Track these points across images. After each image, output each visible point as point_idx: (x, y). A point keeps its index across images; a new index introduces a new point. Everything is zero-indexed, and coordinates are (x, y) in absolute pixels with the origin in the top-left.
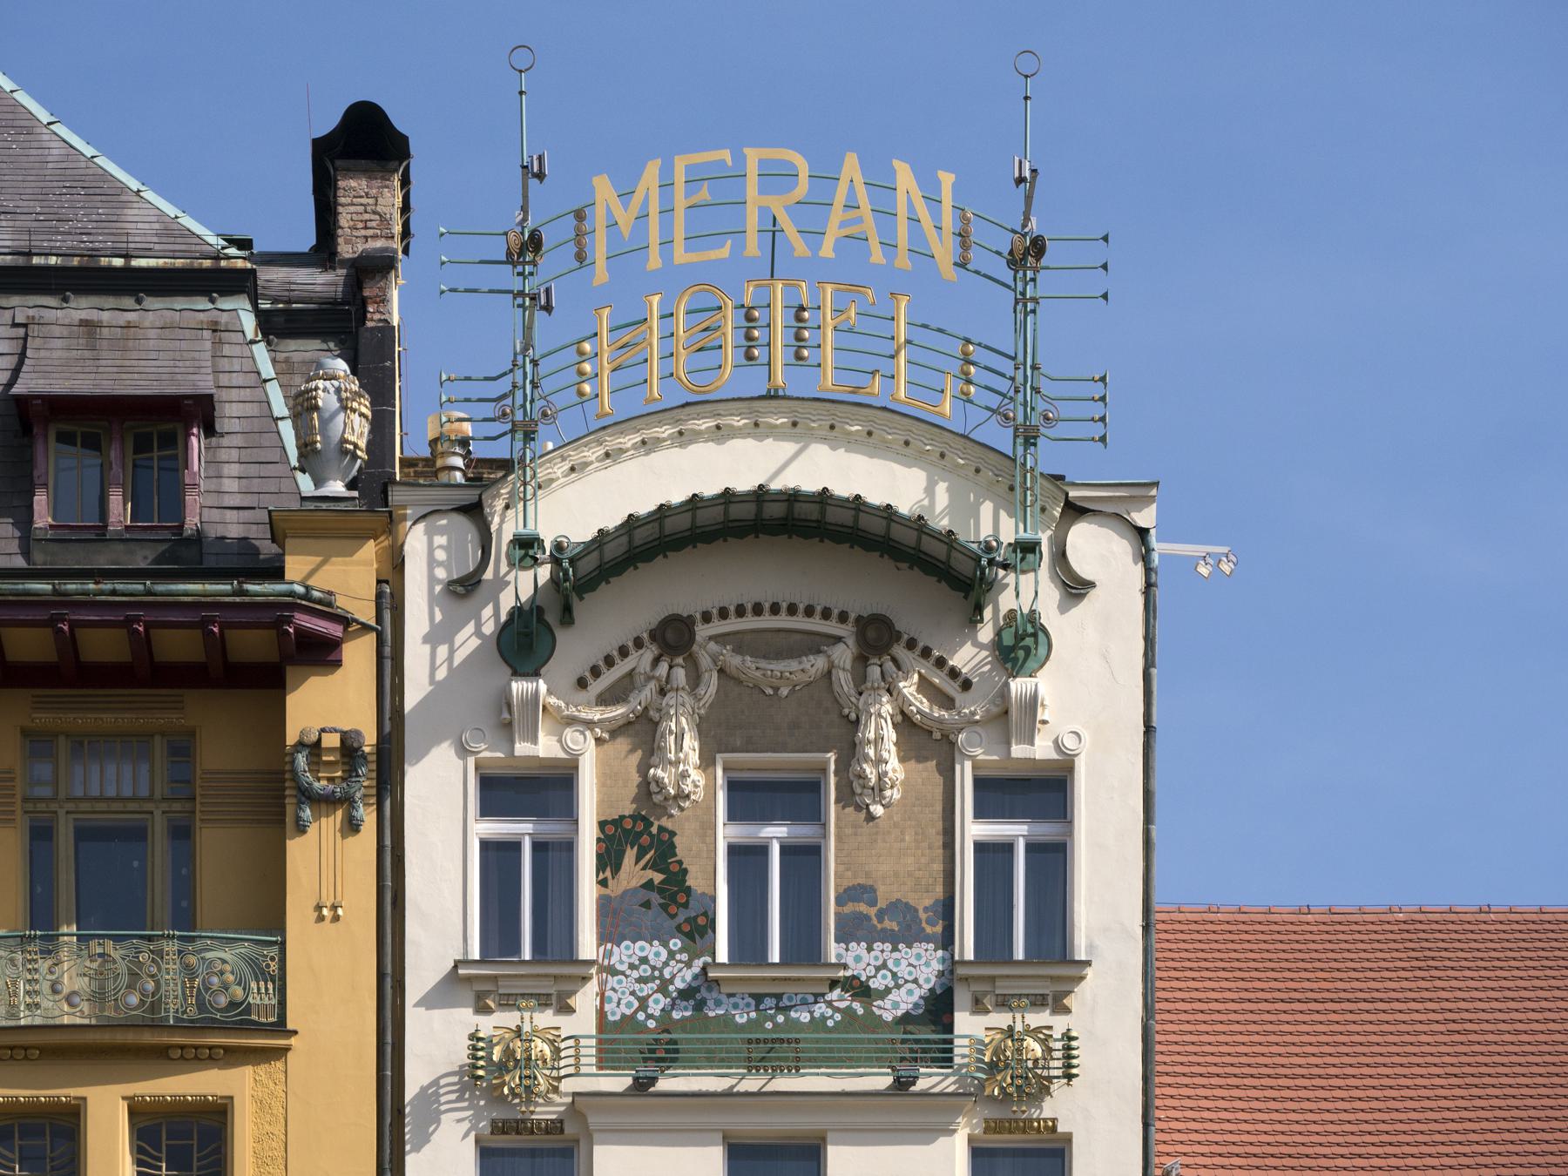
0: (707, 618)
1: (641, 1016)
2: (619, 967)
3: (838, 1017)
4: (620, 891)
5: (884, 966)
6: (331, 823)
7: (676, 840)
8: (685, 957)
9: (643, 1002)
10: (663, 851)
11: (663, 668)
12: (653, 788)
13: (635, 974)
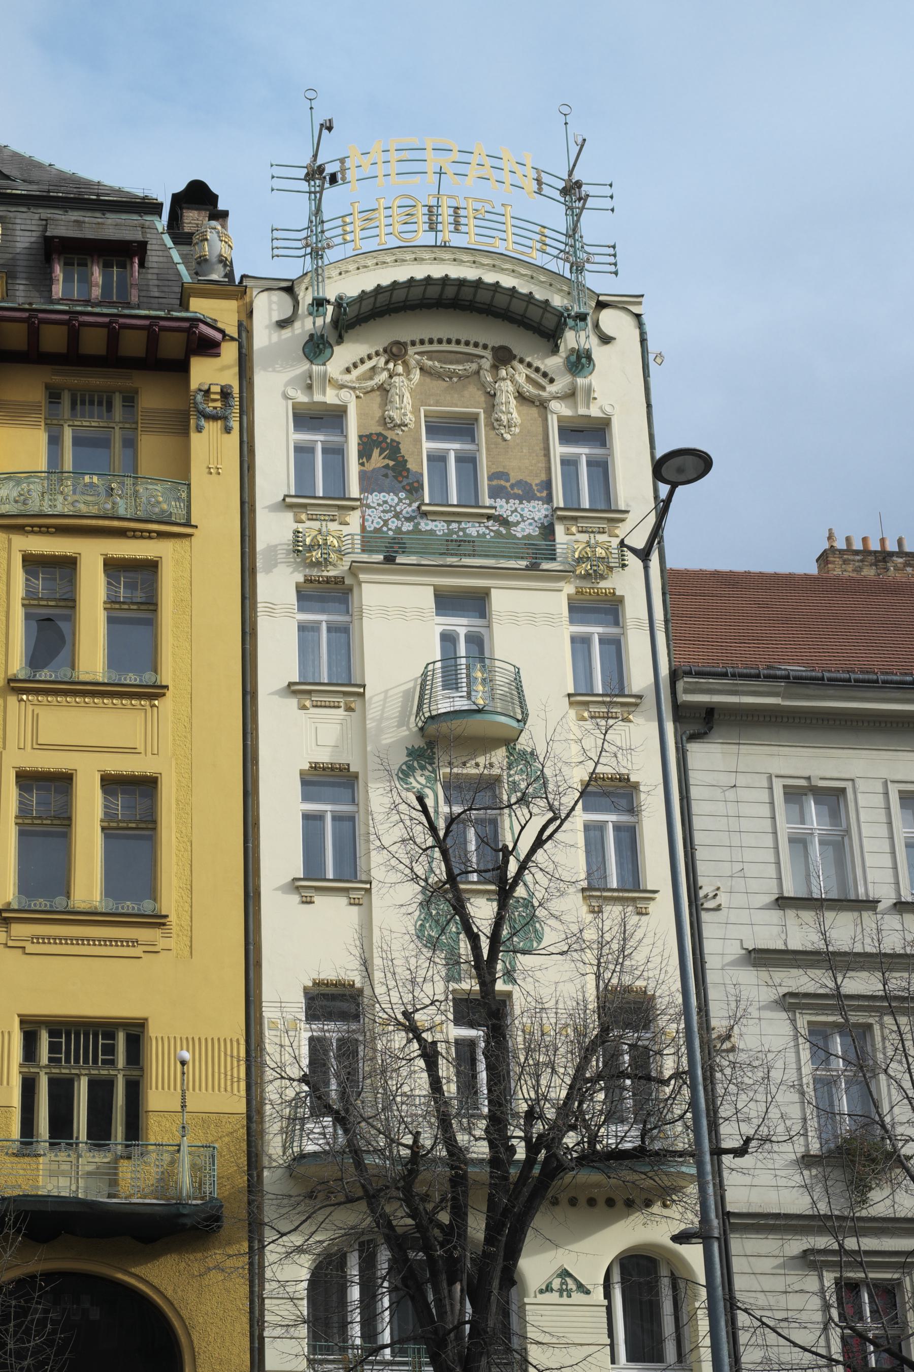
0: (413, 343)
1: (385, 529)
2: (372, 504)
3: (492, 534)
4: (371, 469)
5: (516, 510)
6: (213, 428)
7: (401, 446)
8: (407, 501)
9: (386, 522)
10: (393, 450)
11: (391, 365)
12: (388, 420)
13: (381, 509)
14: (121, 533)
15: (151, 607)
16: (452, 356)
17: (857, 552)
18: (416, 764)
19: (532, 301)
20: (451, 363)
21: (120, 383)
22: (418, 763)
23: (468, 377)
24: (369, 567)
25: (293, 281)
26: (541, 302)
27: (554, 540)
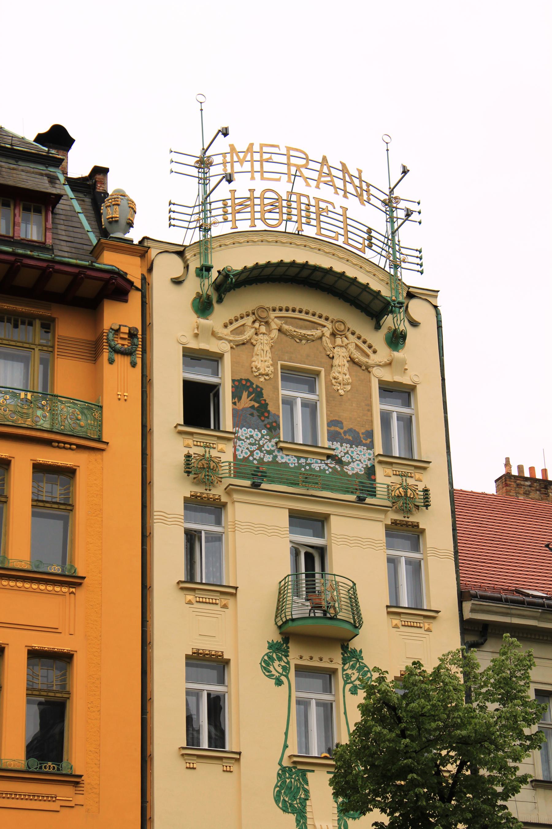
0: (274, 310)
1: (251, 458)
2: (241, 437)
3: (330, 470)
4: (241, 408)
5: (347, 453)
6: (122, 362)
7: (263, 391)
8: (268, 437)
9: (252, 453)
10: (258, 394)
11: (257, 325)
12: (254, 369)
13: (248, 441)
14: (48, 443)
15: (69, 508)
16: (301, 322)
17: (526, 479)
18: (274, 656)
19: (367, 290)
20: (301, 328)
21: (41, 312)
22: (276, 655)
23: (313, 341)
24: (241, 490)
25: (186, 247)
26: (375, 292)
27: (375, 480)
